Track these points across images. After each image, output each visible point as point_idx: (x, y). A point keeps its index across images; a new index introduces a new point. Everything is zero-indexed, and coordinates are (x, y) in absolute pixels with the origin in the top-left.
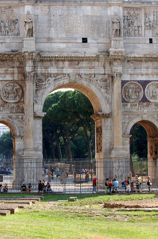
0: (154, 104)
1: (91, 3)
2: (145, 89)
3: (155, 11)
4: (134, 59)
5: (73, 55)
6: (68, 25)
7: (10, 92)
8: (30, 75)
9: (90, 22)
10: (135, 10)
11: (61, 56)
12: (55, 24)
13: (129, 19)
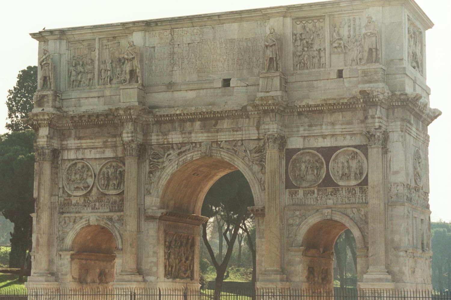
0: (347, 189)
1: (236, 17)
3: (351, 18)
5: (204, 110)
7: (111, 177)
8: (129, 147)
11: (185, 112)
12: (180, 60)
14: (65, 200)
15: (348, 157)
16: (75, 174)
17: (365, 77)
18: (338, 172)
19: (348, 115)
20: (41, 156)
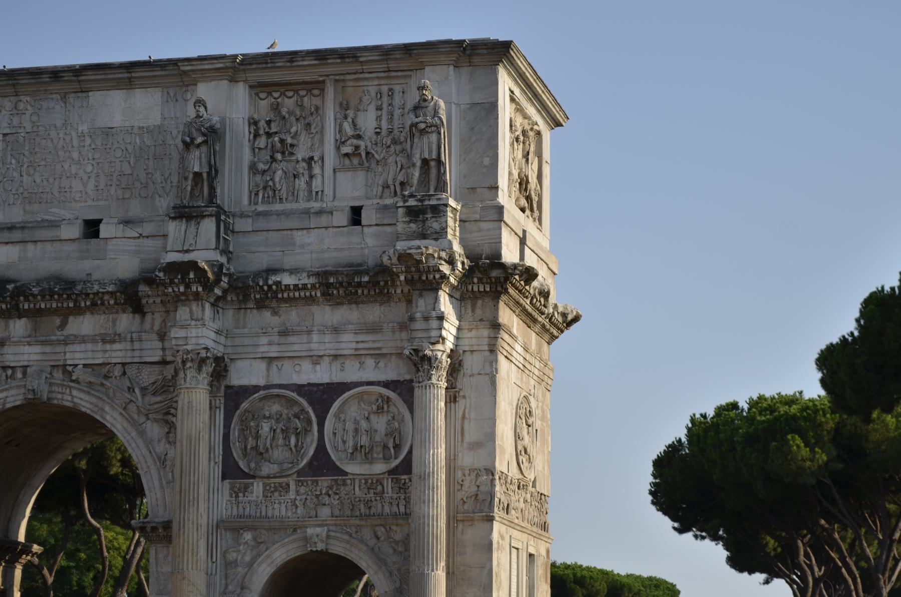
0: (363, 481)
1: (117, 76)
2: (325, 418)
3: (385, 89)
4: (280, 296)
6: (32, 172)
9: (119, 153)
15: (370, 408)
17: (412, 225)
18: (344, 442)
19: (374, 312)
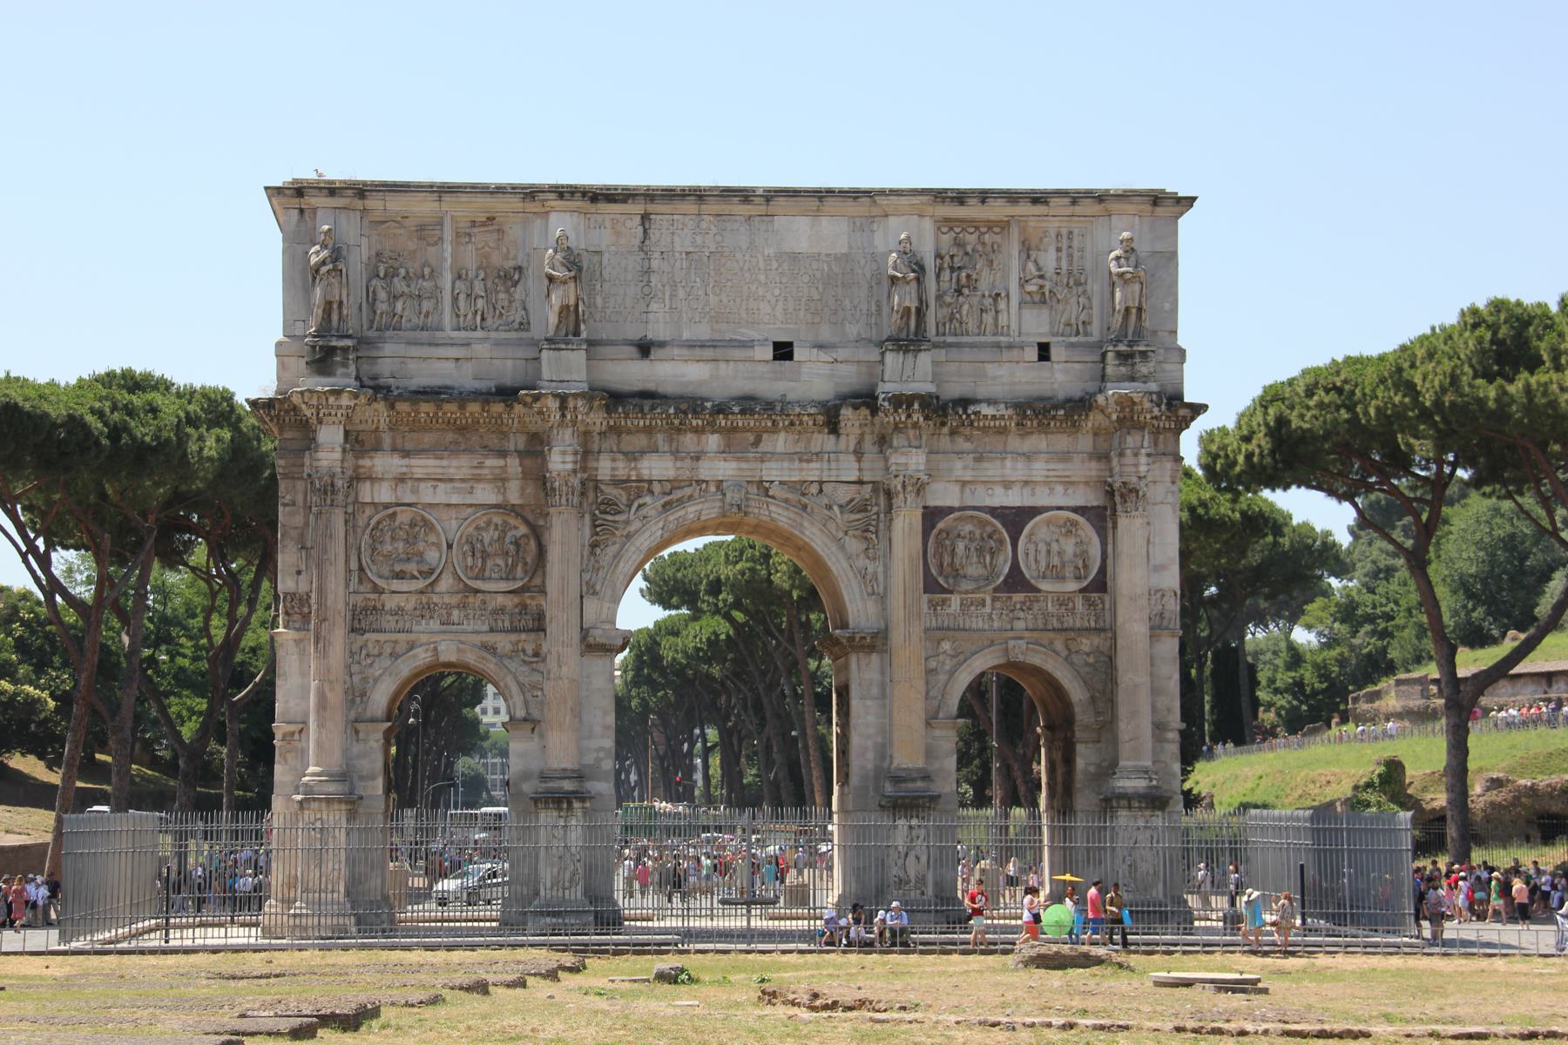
3: (1064, 232)
7: (489, 550)
10: (985, 230)
12: (667, 288)
13: (959, 268)
14: (365, 599)
16: (393, 539)
19: (1062, 442)
20: (326, 494)
